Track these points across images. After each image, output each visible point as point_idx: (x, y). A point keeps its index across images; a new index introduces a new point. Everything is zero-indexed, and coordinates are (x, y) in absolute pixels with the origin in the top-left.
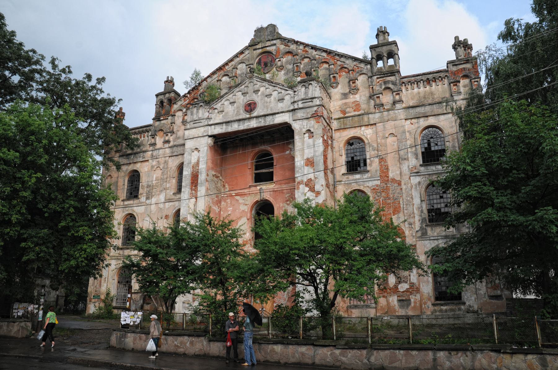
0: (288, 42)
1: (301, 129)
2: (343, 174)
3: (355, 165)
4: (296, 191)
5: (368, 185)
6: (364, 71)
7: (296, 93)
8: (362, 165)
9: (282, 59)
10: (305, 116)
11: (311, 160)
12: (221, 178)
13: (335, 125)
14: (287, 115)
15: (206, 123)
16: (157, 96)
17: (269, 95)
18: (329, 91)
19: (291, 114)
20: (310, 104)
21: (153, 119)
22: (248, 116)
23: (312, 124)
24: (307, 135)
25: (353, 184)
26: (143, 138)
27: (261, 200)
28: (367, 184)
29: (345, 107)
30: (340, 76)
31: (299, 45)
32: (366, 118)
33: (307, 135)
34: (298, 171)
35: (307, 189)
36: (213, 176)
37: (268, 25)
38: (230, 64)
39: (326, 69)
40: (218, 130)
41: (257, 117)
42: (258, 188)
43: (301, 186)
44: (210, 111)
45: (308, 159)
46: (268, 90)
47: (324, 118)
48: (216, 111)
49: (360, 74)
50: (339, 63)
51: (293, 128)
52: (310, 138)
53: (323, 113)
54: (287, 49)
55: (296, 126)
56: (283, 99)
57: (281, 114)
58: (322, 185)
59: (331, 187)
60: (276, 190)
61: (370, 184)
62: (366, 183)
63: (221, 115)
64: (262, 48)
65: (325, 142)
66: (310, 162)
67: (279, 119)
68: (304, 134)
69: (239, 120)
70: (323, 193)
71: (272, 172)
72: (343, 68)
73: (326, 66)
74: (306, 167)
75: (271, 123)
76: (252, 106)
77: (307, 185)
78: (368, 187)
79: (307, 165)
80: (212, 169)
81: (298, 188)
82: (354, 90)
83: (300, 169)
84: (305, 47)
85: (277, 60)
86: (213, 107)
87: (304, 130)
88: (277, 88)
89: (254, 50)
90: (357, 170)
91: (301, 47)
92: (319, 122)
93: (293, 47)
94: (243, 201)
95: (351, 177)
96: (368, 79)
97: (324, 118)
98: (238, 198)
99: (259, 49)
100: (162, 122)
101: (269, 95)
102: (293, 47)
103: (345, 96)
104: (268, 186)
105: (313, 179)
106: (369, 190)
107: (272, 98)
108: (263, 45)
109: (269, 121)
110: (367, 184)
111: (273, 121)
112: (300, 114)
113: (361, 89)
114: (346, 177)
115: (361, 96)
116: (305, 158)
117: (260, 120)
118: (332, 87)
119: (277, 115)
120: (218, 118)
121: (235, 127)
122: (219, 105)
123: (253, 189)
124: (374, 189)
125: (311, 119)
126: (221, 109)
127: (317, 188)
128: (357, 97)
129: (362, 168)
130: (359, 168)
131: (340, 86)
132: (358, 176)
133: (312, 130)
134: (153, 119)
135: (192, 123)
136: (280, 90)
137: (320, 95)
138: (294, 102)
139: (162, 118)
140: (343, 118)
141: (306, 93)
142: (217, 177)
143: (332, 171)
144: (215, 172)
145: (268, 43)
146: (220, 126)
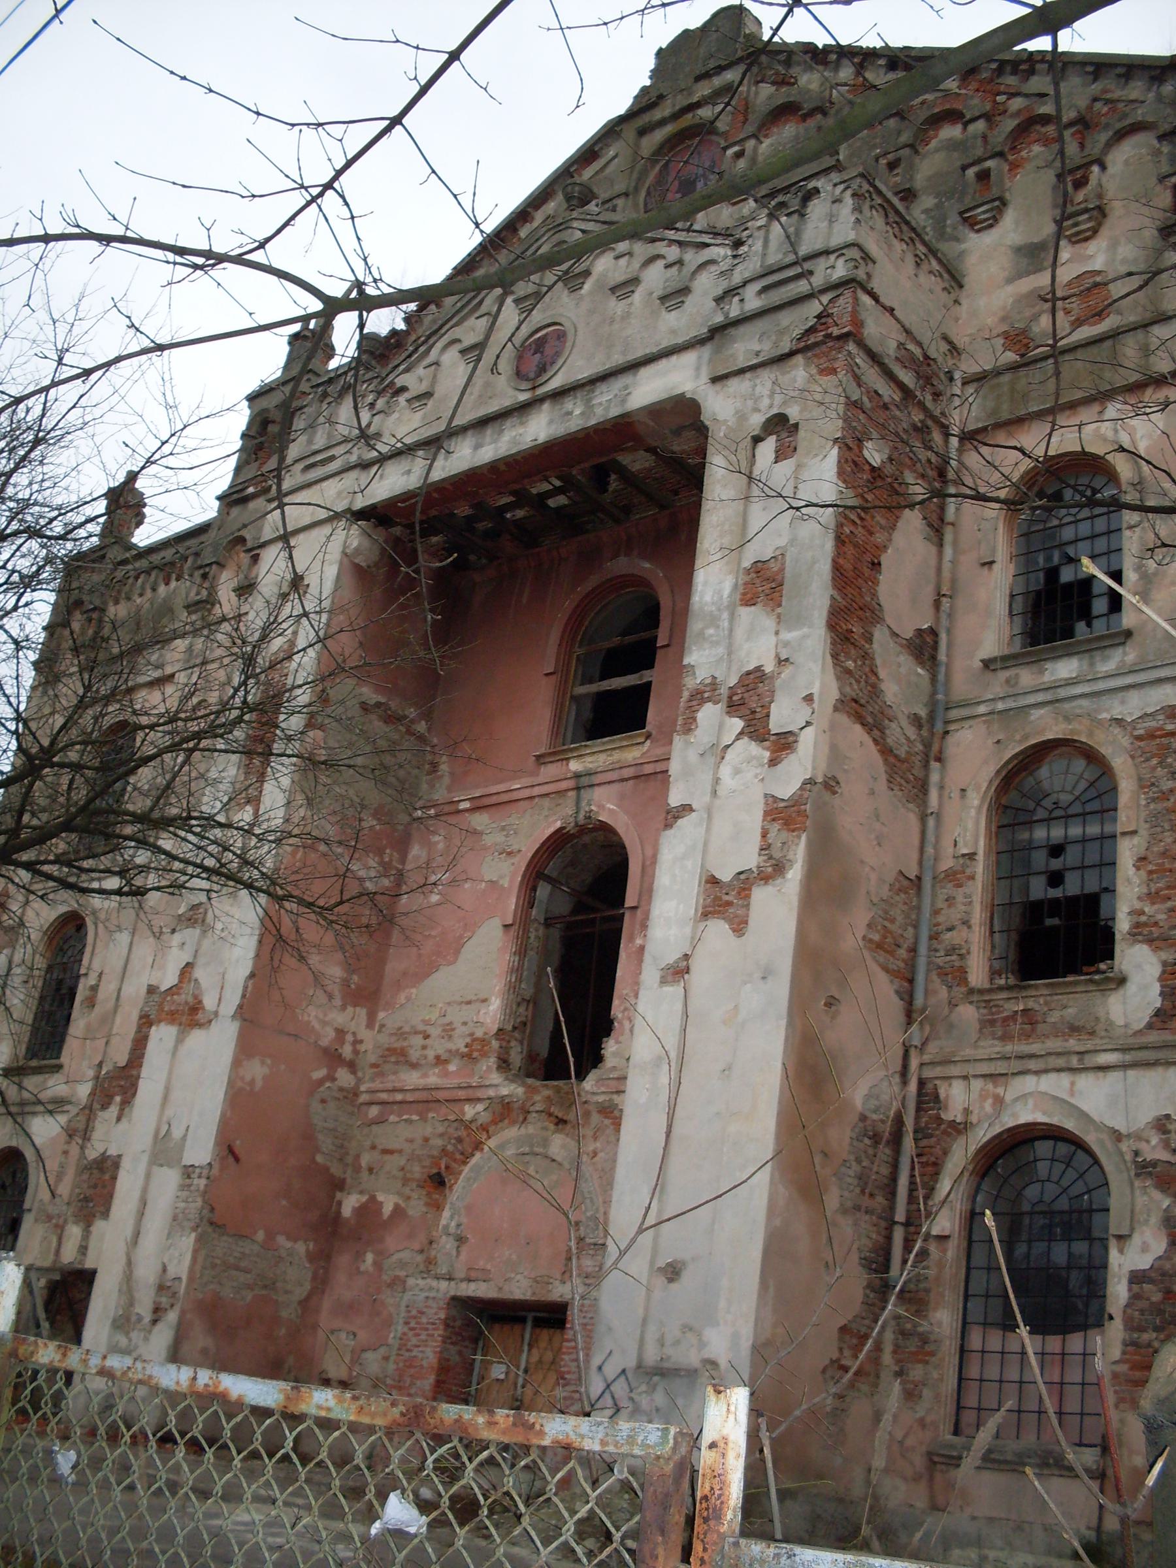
0: (788, 63)
1: (741, 417)
2: (987, 664)
3: (1059, 611)
4: (678, 741)
5: (1117, 711)
6: (1140, 114)
7: (744, 249)
8: (1100, 605)
9: (751, 143)
10: (767, 349)
11: (774, 566)
12: (422, 727)
13: (966, 410)
14: (689, 358)
15: (353, 458)
16: (252, 398)
17: (624, 288)
18: (947, 248)
19: (706, 351)
20: (802, 287)
21: (219, 498)
22: (523, 397)
23: (804, 391)
24: (767, 448)
25: (1036, 714)
26: (173, 584)
27: (582, 830)
28: (1117, 708)
29: (1028, 313)
30: (1014, 166)
31: (837, 66)
32: (1129, 349)
33: (767, 448)
34: (701, 634)
35: (737, 724)
36: (365, 707)
37: (715, 16)
38: (539, 217)
39: (953, 146)
40: (392, 482)
41: (558, 395)
42: (574, 766)
43: (709, 714)
44: (380, 404)
45: (759, 568)
46: (623, 262)
47: (874, 357)
48: (402, 399)
49: (1121, 135)
50: (1017, 104)
51: (706, 418)
52: (780, 456)
53: (858, 323)
54: (784, 95)
55: (722, 408)
56: (685, 291)
57: (663, 364)
58: (809, 699)
59: (901, 733)
60: (648, 769)
61: (1132, 706)
62: (1106, 701)
63: (419, 415)
64: (675, 116)
65: (852, 465)
66: (764, 585)
67: (648, 389)
68: (757, 440)
69: (482, 423)
70: (807, 739)
71: (649, 684)
72: (1029, 124)
73: (951, 132)
74: (745, 612)
75: (615, 412)
76: (549, 350)
77: (734, 706)
78: (1119, 722)
79: (749, 600)
80: (361, 672)
81: (689, 725)
82: (1078, 217)
83: (714, 621)
84: (860, 68)
85: (730, 152)
86: (392, 383)
87: (756, 421)
88: (661, 248)
89: (642, 132)
90: (1069, 633)
91: (846, 73)
92: (834, 371)
93: (810, 81)
94: (499, 838)
95: (1026, 677)
96: (1157, 153)
97: (874, 357)
98: (480, 821)
99: (662, 123)
100: (252, 505)
101: (624, 288)
102: (810, 81)
103: (1034, 255)
104: (617, 756)
105: (769, 668)
106: (1125, 741)
107: (638, 297)
108: (682, 101)
109: (606, 404)
110: (1117, 708)
111: (624, 401)
112: (746, 346)
113: (1117, 209)
114: (1003, 675)
115: (1114, 245)
116: (747, 564)
117: (569, 404)
118: (972, 223)
119: (644, 372)
120: (403, 424)
121: (465, 456)
122: (420, 371)
123: (551, 771)
124: (1151, 735)
125: (799, 359)
126: (423, 388)
127: (784, 714)
128: (1096, 256)
129: (1099, 626)
130: (1081, 627)
131: (1009, 218)
132: (1065, 668)
133: (794, 413)
134: (219, 498)
135: (300, 466)
136: (673, 253)
137: (851, 236)
138: (731, 292)
139: (251, 490)
140: (1014, 368)
141: (792, 241)
142: (391, 719)
143: (925, 647)
144: (378, 689)
145: (704, 89)
146: (403, 464)
